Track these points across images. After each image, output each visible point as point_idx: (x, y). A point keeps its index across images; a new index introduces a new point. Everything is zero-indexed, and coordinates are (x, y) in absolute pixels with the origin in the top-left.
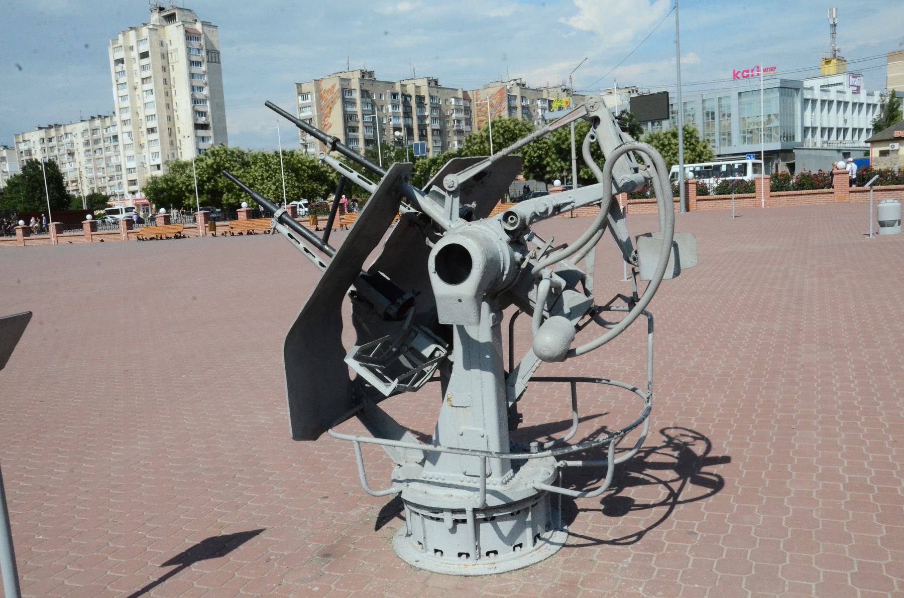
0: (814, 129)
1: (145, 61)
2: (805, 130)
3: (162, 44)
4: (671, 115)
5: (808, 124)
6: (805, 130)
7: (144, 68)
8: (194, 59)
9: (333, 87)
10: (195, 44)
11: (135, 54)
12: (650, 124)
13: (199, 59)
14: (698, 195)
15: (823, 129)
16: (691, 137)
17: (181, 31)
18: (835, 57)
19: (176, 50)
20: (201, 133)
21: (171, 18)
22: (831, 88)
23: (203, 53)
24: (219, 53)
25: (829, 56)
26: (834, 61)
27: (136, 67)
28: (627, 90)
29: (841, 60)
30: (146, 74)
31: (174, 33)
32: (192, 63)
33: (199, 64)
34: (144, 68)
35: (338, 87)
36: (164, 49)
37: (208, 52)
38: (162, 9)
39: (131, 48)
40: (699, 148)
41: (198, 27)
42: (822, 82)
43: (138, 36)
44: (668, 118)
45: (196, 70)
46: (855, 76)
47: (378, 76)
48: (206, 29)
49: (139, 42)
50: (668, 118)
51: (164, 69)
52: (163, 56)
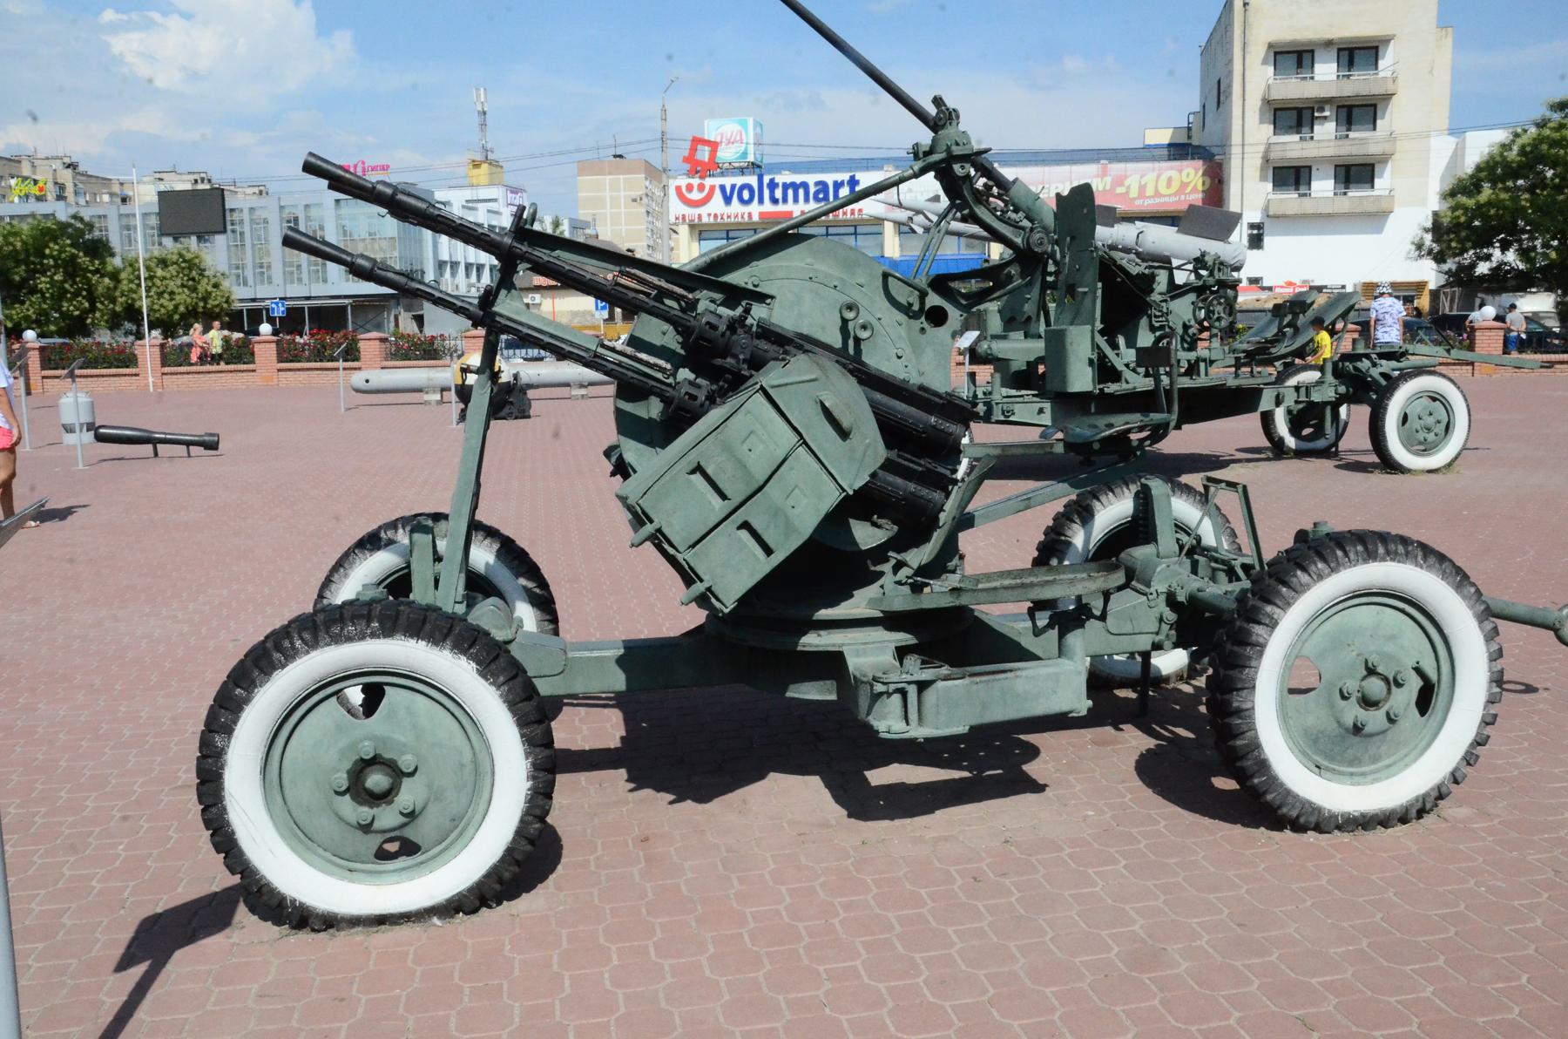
0: (455, 265)
2: (441, 265)
4: (229, 227)
5: (445, 256)
6: (441, 265)
14: (43, 368)
15: (468, 266)
16: (190, 269)
18: (486, 159)
22: (480, 205)
25: (479, 157)
26: (485, 166)
29: (494, 164)
40: (204, 286)
42: (468, 194)
44: (224, 231)
46: (515, 191)
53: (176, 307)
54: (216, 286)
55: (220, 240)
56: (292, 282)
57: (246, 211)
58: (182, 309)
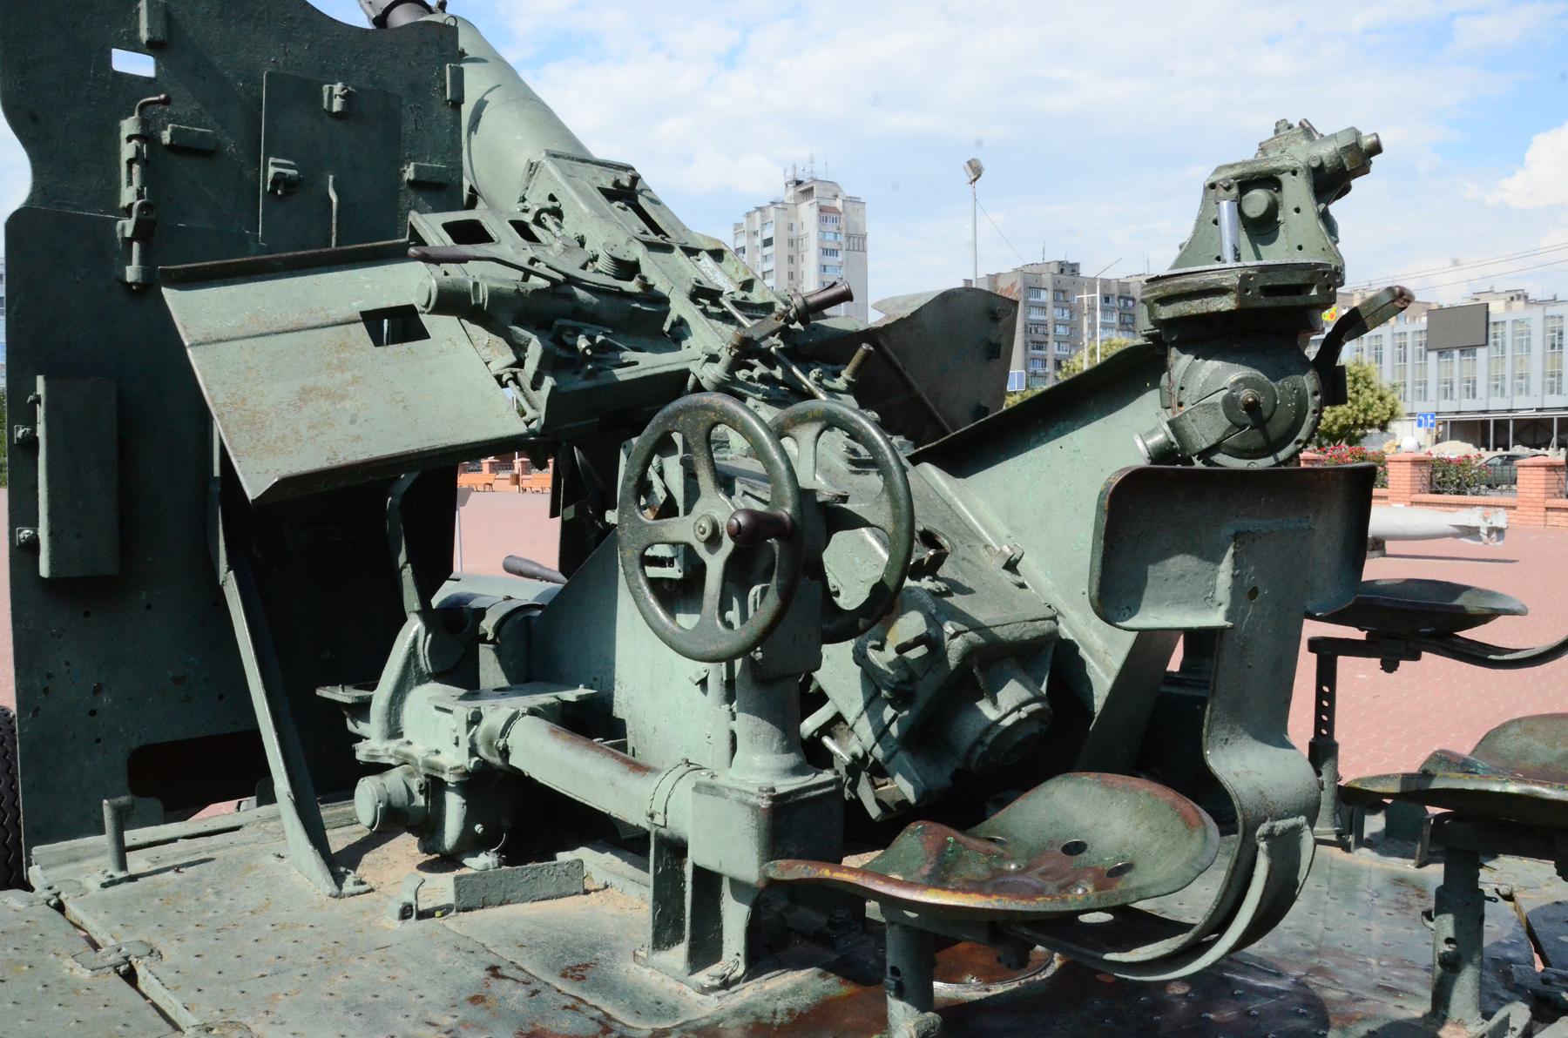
1: (768, 250)
3: (791, 227)
4: (1491, 340)
7: (765, 258)
8: (829, 246)
9: (1013, 285)
10: (831, 227)
11: (758, 241)
12: (1456, 353)
13: (835, 247)
17: (815, 210)
19: (807, 235)
21: (808, 192)
23: (842, 238)
24: (864, 237)
27: (759, 257)
28: (1508, 296)
30: (767, 267)
31: (808, 212)
32: (826, 252)
33: (834, 252)
34: (765, 258)
35: (1019, 285)
36: (794, 234)
37: (848, 237)
38: (799, 183)
39: (755, 233)
41: (838, 204)
43: (763, 218)
45: (829, 260)
47: (1085, 272)
48: (849, 205)
49: (764, 225)
50: (1487, 343)
51: (791, 259)
52: (791, 242)
53: (1336, 419)
54: (1381, 398)
55: (1481, 352)
56: (1552, 392)
57: (1509, 324)
58: (1341, 420)
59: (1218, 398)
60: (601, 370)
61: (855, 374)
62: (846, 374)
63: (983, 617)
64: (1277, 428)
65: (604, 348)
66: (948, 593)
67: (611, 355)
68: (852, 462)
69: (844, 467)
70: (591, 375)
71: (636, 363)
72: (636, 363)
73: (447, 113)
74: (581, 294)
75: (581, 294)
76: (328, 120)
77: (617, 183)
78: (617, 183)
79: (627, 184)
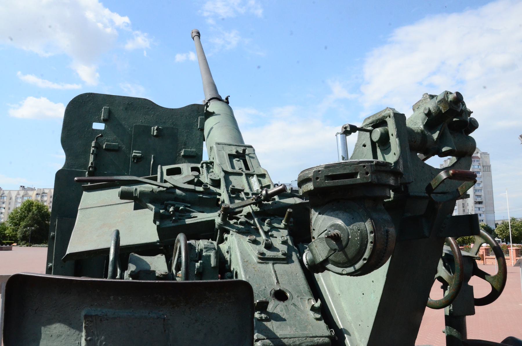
20: (480, 206)
59: (323, 235)
60: (181, 219)
61: (286, 222)
62: (283, 222)
63: (279, 333)
64: (351, 251)
65: (184, 211)
66: (267, 320)
67: (187, 214)
68: (260, 258)
69: (255, 260)
70: (174, 221)
71: (196, 217)
72: (196, 217)
73: (199, 132)
74: (178, 192)
75: (178, 192)
76: (153, 138)
77: (237, 152)
78: (237, 152)
79: (241, 152)
